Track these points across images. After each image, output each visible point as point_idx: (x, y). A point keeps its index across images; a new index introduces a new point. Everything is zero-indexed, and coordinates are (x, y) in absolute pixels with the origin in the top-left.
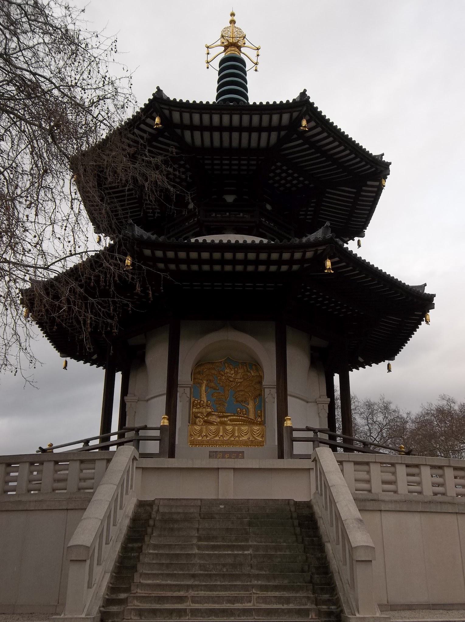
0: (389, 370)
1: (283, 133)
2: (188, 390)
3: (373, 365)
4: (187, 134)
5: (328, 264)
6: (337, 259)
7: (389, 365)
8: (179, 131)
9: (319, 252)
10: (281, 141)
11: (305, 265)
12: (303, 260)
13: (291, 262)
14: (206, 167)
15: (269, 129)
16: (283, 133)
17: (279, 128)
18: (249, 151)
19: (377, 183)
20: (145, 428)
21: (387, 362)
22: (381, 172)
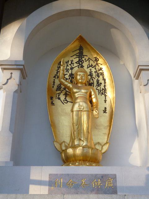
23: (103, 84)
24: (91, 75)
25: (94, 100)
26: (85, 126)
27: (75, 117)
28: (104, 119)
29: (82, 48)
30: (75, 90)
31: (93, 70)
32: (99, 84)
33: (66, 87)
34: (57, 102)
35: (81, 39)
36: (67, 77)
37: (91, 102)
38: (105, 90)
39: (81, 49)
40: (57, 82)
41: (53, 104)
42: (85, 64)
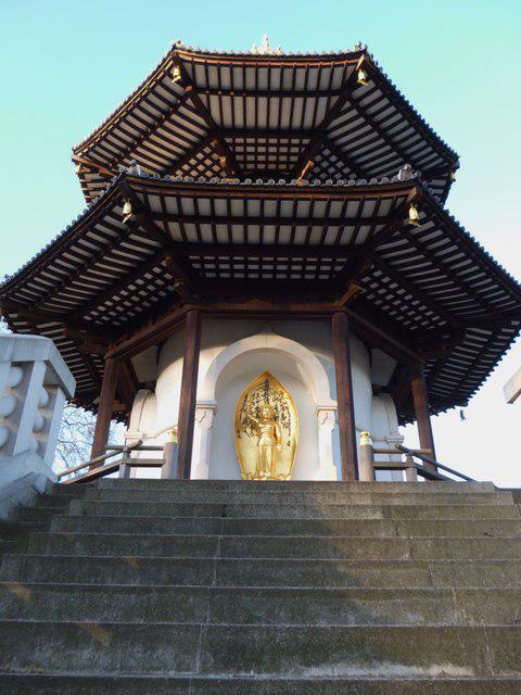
0: (463, 418)
1: (335, 99)
2: (210, 413)
3: (441, 414)
4: (214, 99)
5: (413, 214)
6: (423, 215)
7: (461, 412)
8: (203, 97)
9: (400, 200)
10: (333, 113)
11: (379, 227)
12: (373, 220)
13: (358, 221)
14: (239, 158)
15: (317, 93)
16: (335, 99)
17: (329, 93)
18: (290, 132)
19: (443, 183)
20: (138, 447)
21: (458, 408)
22: (451, 164)
23: (287, 420)
24: (276, 408)
25: (278, 435)
26: (269, 459)
27: (261, 452)
28: (287, 452)
29: (268, 382)
30: (261, 425)
31: (279, 403)
32: (284, 418)
33: (251, 421)
34: (243, 435)
35: (267, 374)
36: (253, 410)
37: (275, 436)
38: (289, 423)
39: (267, 382)
40: (244, 415)
41: (239, 437)
42: (271, 398)
